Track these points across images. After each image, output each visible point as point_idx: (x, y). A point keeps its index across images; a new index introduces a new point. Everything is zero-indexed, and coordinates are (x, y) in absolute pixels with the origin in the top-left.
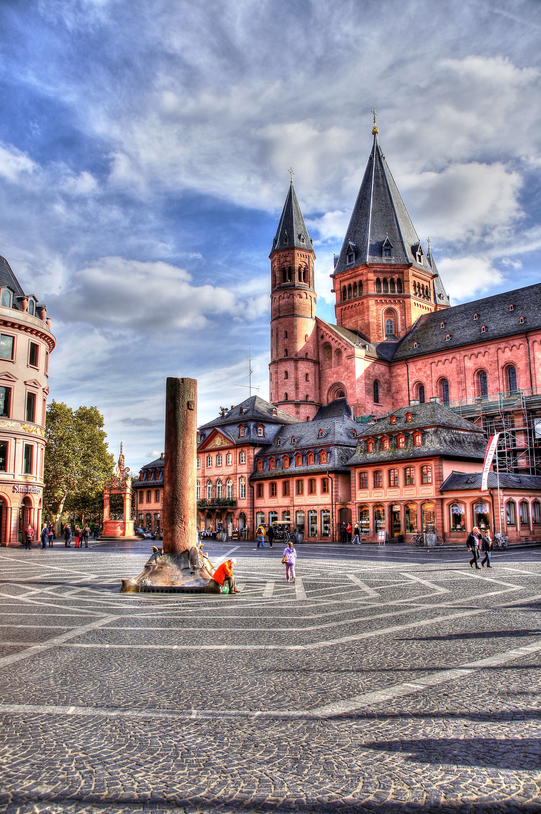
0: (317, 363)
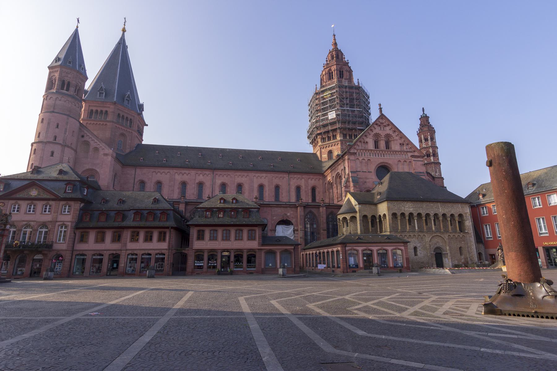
0: (76, 151)
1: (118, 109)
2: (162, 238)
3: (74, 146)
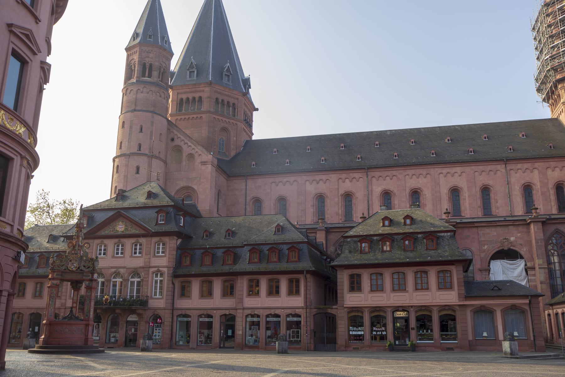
0: (165, 162)
1: (216, 92)
2: (294, 290)
3: (162, 156)
